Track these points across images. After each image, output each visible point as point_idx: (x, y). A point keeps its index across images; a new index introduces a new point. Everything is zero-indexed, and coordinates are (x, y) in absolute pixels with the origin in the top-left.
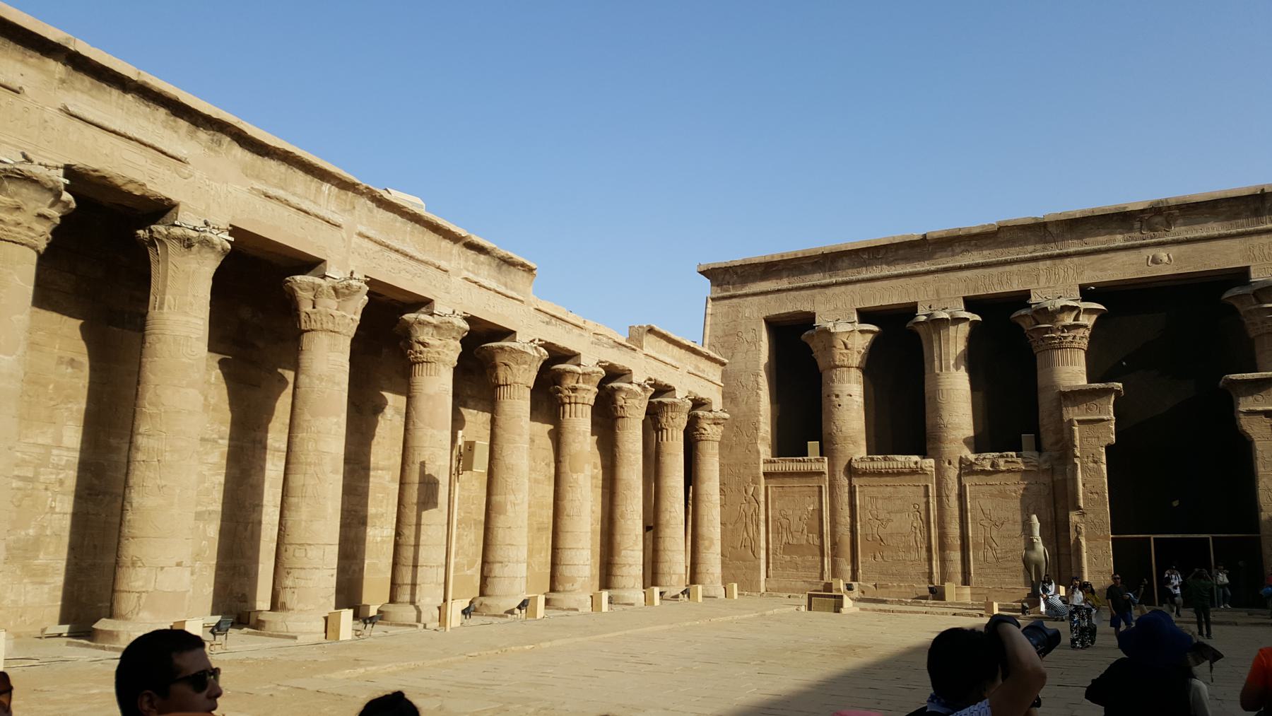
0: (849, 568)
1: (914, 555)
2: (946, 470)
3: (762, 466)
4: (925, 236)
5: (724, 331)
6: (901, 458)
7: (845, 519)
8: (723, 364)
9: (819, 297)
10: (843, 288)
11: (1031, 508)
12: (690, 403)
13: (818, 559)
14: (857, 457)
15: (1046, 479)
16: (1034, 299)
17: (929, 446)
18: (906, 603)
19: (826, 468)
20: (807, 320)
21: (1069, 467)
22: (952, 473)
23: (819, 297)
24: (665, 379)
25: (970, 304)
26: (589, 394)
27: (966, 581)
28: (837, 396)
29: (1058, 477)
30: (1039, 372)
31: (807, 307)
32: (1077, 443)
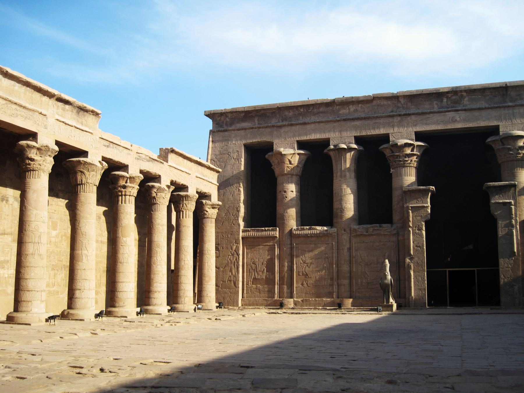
4: (334, 100)
5: (220, 151)
6: (319, 228)
8: (218, 172)
9: (275, 133)
10: (289, 128)
11: (387, 255)
12: (197, 196)
15: (394, 239)
18: (319, 309)
20: (269, 147)
21: (406, 232)
23: (275, 133)
24: (181, 180)
26: (133, 189)
29: (401, 238)
30: (393, 179)
32: (411, 219)
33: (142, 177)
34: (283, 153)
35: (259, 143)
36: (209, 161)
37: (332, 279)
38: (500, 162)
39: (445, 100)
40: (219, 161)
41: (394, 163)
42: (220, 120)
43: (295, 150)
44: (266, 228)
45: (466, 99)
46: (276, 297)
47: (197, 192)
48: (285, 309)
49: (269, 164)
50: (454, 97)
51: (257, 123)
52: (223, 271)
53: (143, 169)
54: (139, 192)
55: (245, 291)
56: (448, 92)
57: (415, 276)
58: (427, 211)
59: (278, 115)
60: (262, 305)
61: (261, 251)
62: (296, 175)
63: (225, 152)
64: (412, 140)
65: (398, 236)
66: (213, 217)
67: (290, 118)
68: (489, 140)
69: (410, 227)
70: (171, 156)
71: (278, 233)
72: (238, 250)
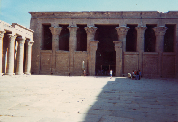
11: (84, 60)
12: (25, 39)
16: (87, 26)
17: (69, 49)
20: (50, 25)
24: (20, 34)
25: (78, 25)
29: (88, 55)
31: (50, 23)
33: (5, 32)
35: (47, 24)
37: (68, 66)
38: (118, 35)
39: (104, 15)
45: (110, 15)
47: (26, 38)
49: (50, 31)
50: (107, 14)
53: (5, 29)
54: (4, 37)
56: (105, 13)
62: (58, 35)
65: (88, 54)
68: (116, 28)
70: (16, 26)
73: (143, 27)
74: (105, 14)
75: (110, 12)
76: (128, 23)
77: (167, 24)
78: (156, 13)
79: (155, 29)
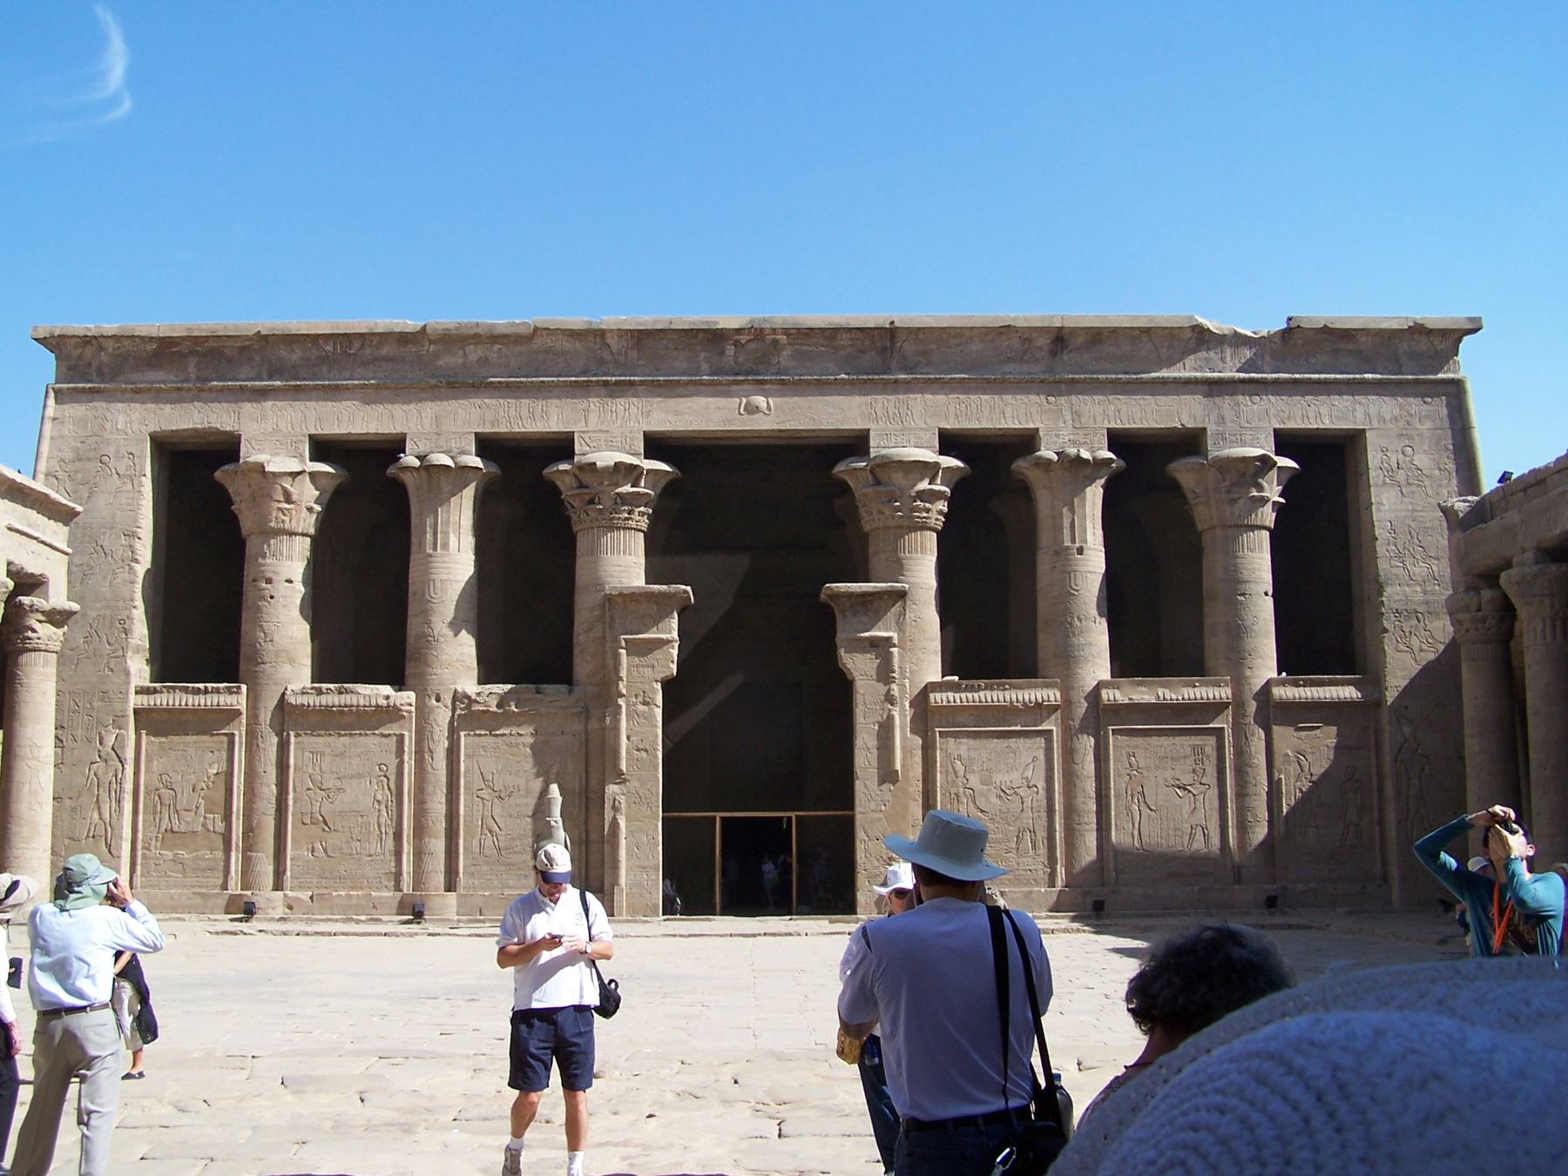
0: (271, 868)
1: (375, 847)
2: (432, 710)
3: (132, 696)
7: (269, 790)
12: (11, 584)
13: (220, 855)
14: (297, 687)
17: (410, 669)
18: (358, 922)
19: (240, 701)
20: (226, 449)
21: (609, 710)
22: (442, 716)
25: (487, 445)
27: (450, 886)
28: (269, 581)
29: (594, 725)
32: (623, 674)
34: (269, 468)
36: (41, 476)
38: (867, 528)
39: (730, 350)
40: (72, 480)
41: (583, 516)
42: (80, 357)
43: (302, 461)
44: (209, 685)
45: (787, 352)
46: (235, 887)
47: (9, 574)
48: (260, 920)
49: (222, 499)
51: (193, 376)
52: (73, 809)
55: (139, 868)
56: (738, 331)
57: (630, 832)
58: (671, 655)
59: (257, 358)
60: (189, 910)
61: (191, 751)
63: (92, 454)
64: (635, 454)
65: (588, 718)
66: (51, 647)
67: (294, 367)
68: (840, 468)
69: (622, 696)
71: (243, 699)
72: (123, 748)
73: (1085, 455)
74: (737, 344)
75: (786, 331)
76: (951, 424)
77: (1290, 425)
78: (1189, 334)
79: (1183, 471)
